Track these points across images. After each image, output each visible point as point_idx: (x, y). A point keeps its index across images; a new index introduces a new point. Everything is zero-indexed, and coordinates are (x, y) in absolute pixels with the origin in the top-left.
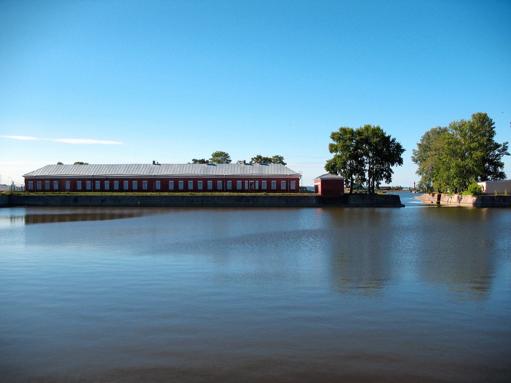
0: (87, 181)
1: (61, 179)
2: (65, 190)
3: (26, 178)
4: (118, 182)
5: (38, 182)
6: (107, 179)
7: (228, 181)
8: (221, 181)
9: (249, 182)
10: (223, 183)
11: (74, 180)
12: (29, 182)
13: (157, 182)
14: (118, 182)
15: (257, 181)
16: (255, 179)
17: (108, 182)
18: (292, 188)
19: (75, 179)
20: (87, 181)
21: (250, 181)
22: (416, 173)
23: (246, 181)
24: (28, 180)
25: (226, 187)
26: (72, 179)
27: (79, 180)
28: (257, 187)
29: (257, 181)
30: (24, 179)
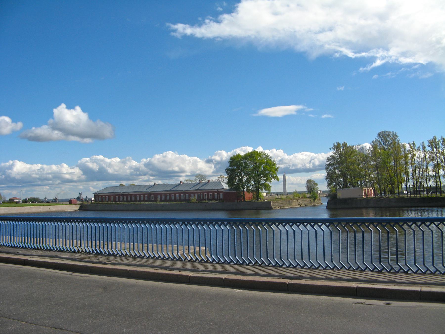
6: (129, 195)
8: (183, 194)
9: (197, 194)
10: (184, 196)
12: (96, 197)
15: (202, 194)
17: (130, 196)
18: (187, 199)
21: (199, 194)
22: (93, 194)
23: (196, 194)
24: (97, 196)
25: (186, 198)
28: (202, 197)
29: (202, 194)
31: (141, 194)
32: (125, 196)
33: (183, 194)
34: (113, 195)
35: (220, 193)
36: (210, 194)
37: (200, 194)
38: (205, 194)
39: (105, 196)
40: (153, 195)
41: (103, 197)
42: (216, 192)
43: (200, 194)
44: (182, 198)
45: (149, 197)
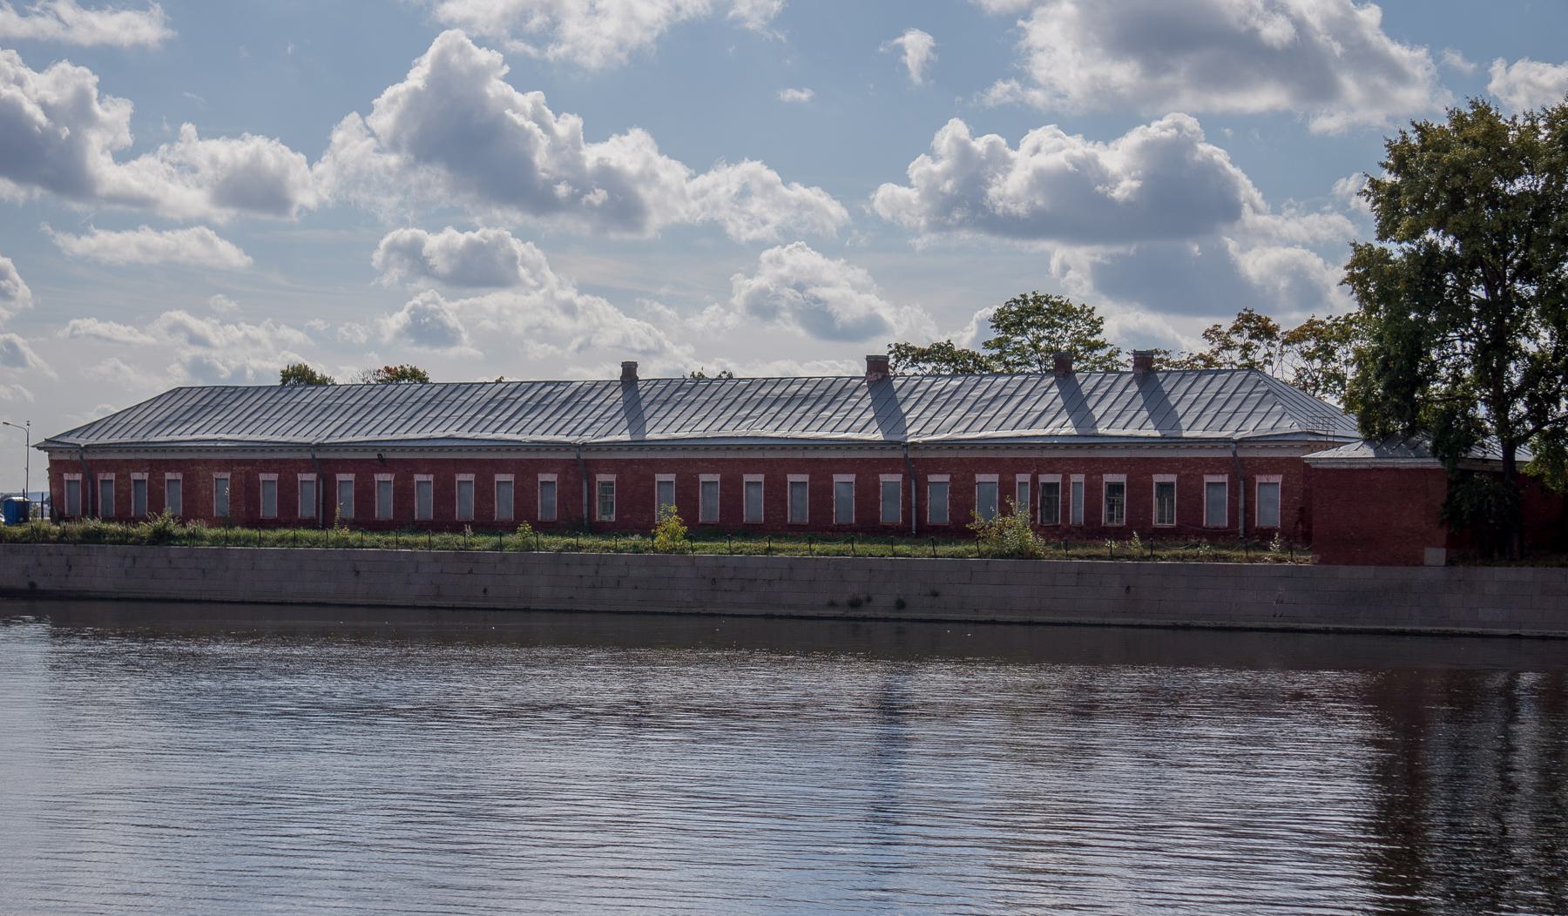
0: (299, 475)
1: (193, 462)
2: (458, 528)
3: (57, 457)
4: (431, 478)
5: (100, 477)
6: (383, 464)
7: (932, 478)
8: (898, 478)
9: (1034, 480)
11: (248, 468)
12: (66, 477)
13: (602, 478)
14: (431, 478)
16: (1066, 466)
17: (389, 477)
19: (253, 462)
20: (299, 475)
21: (1045, 478)
23: (1024, 478)
25: (921, 511)
26: (240, 462)
27: (267, 465)
28: (1078, 514)
29: (1078, 478)
30: (42, 460)
31: (501, 466)
32: (340, 477)
33: (898, 478)
34: (227, 465)
35: (1259, 479)
36: (1158, 478)
37: (1066, 478)
38: (1109, 478)
39: (157, 467)
40: (612, 478)
41: (136, 476)
42: (1216, 466)
43: (1066, 478)
44: (890, 512)
45: (569, 495)
